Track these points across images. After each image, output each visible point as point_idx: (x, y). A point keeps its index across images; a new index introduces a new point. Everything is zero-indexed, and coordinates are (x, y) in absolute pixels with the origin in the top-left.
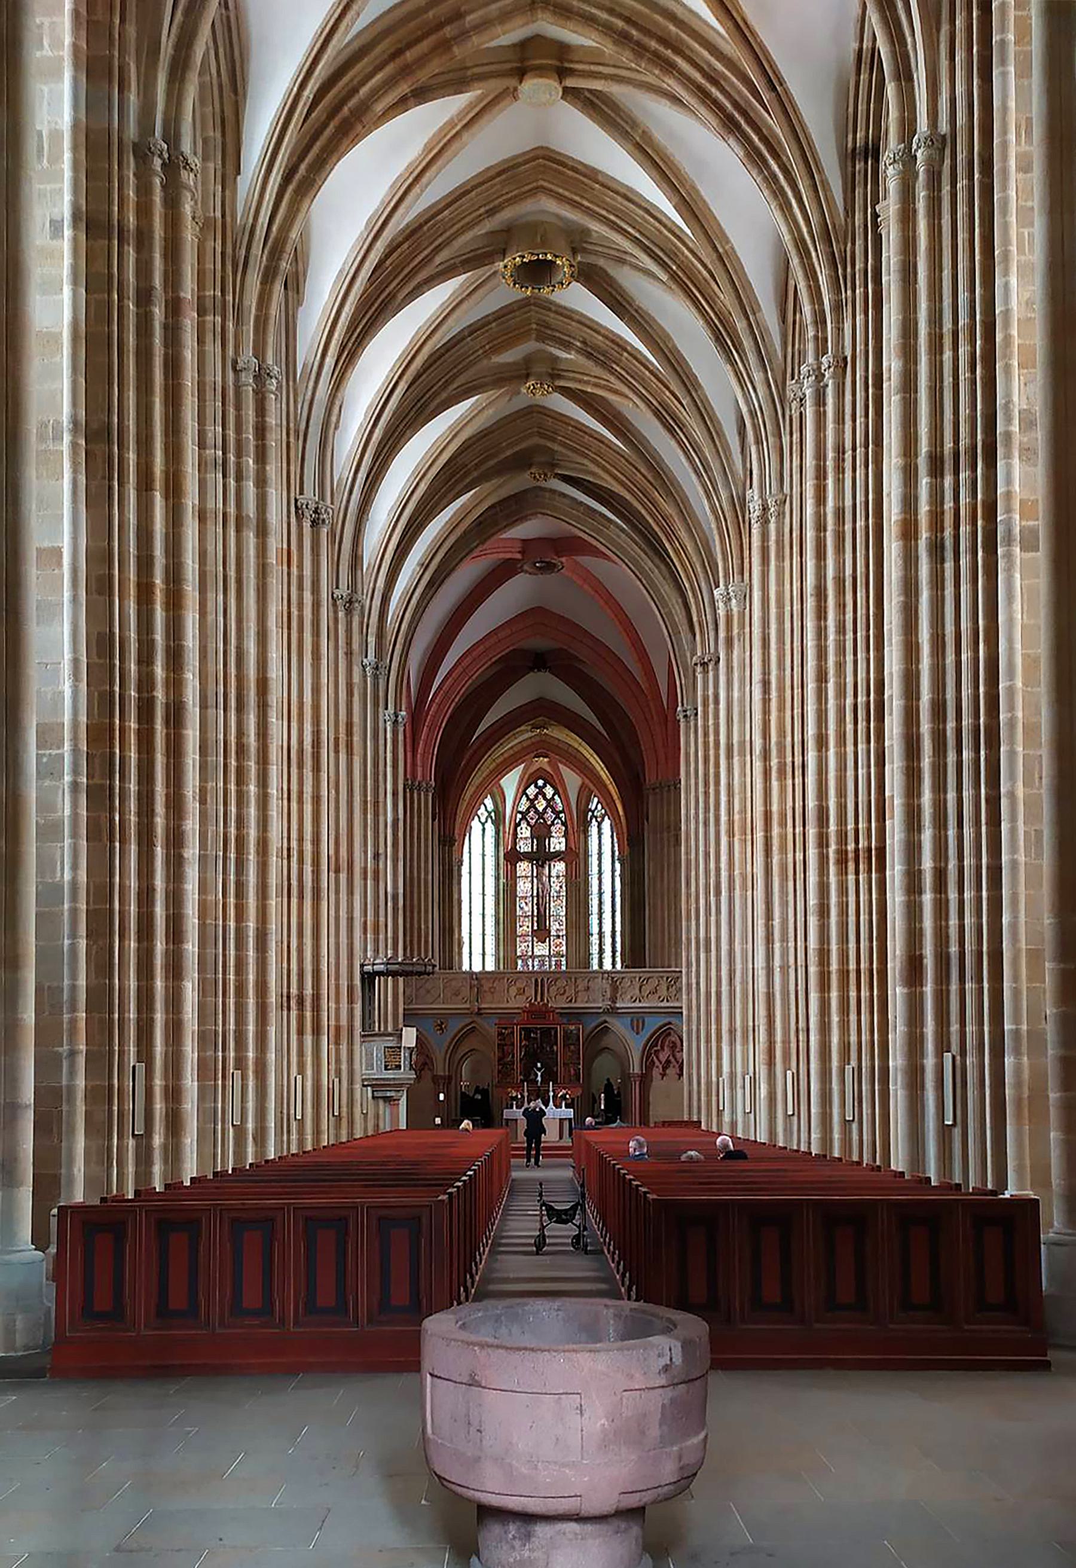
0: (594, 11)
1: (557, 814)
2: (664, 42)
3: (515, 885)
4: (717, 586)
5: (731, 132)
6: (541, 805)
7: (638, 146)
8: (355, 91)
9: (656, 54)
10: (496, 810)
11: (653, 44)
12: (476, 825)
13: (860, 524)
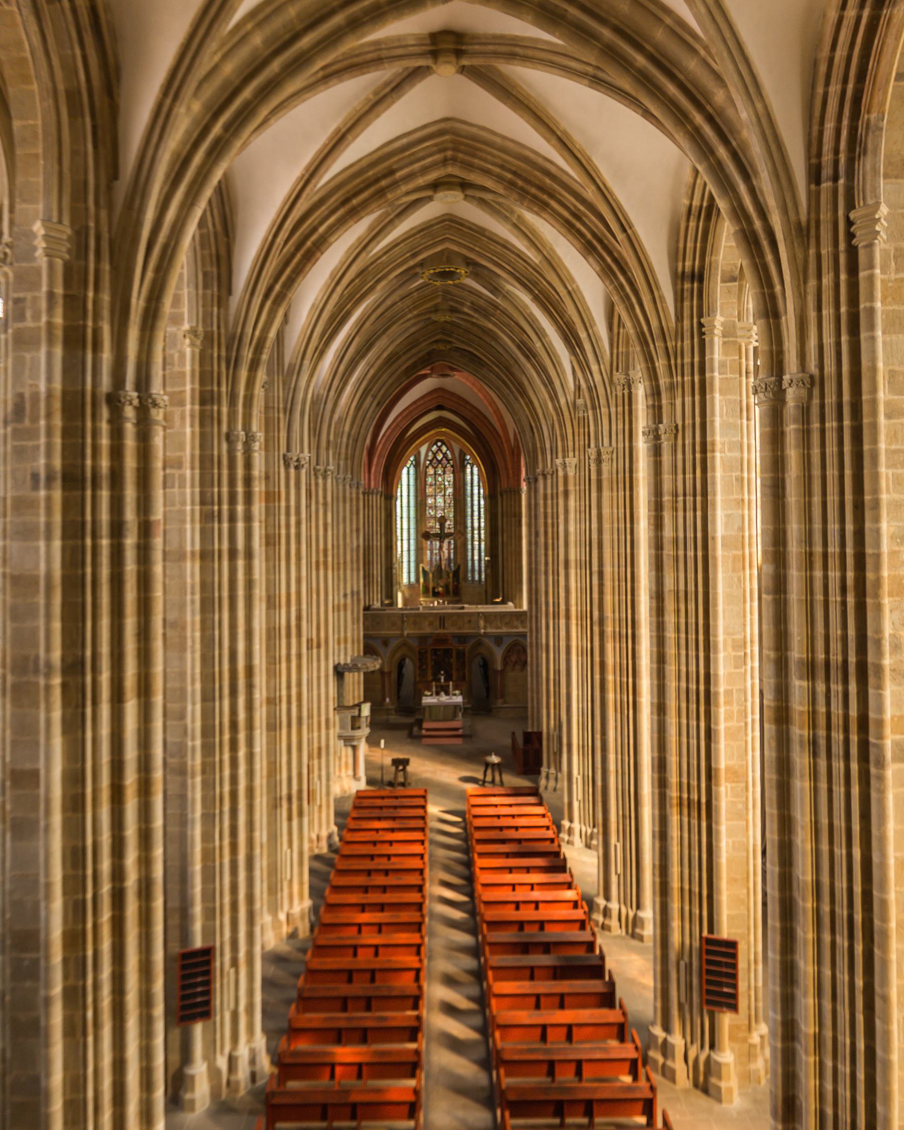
0: (490, 167)
1: (448, 461)
2: (541, 188)
3: (426, 500)
4: (557, 458)
5: (590, 253)
6: (440, 456)
7: (515, 226)
8: (315, 229)
9: (534, 197)
10: (415, 460)
11: (533, 190)
12: (405, 471)
13: (691, 553)
